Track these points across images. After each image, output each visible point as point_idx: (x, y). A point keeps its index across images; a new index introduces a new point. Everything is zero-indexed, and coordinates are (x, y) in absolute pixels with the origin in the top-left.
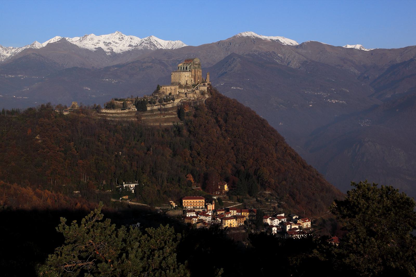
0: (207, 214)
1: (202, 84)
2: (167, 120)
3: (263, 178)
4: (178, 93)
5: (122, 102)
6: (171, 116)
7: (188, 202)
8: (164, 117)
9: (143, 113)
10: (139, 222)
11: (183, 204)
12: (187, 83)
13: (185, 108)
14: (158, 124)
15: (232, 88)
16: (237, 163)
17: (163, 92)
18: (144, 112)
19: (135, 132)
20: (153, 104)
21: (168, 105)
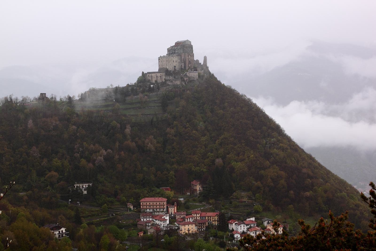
0: (163, 218)
4: (164, 81)
7: (146, 204)
10: (64, 228)
11: (142, 207)
12: (175, 69)
15: (299, 74)
17: (149, 81)
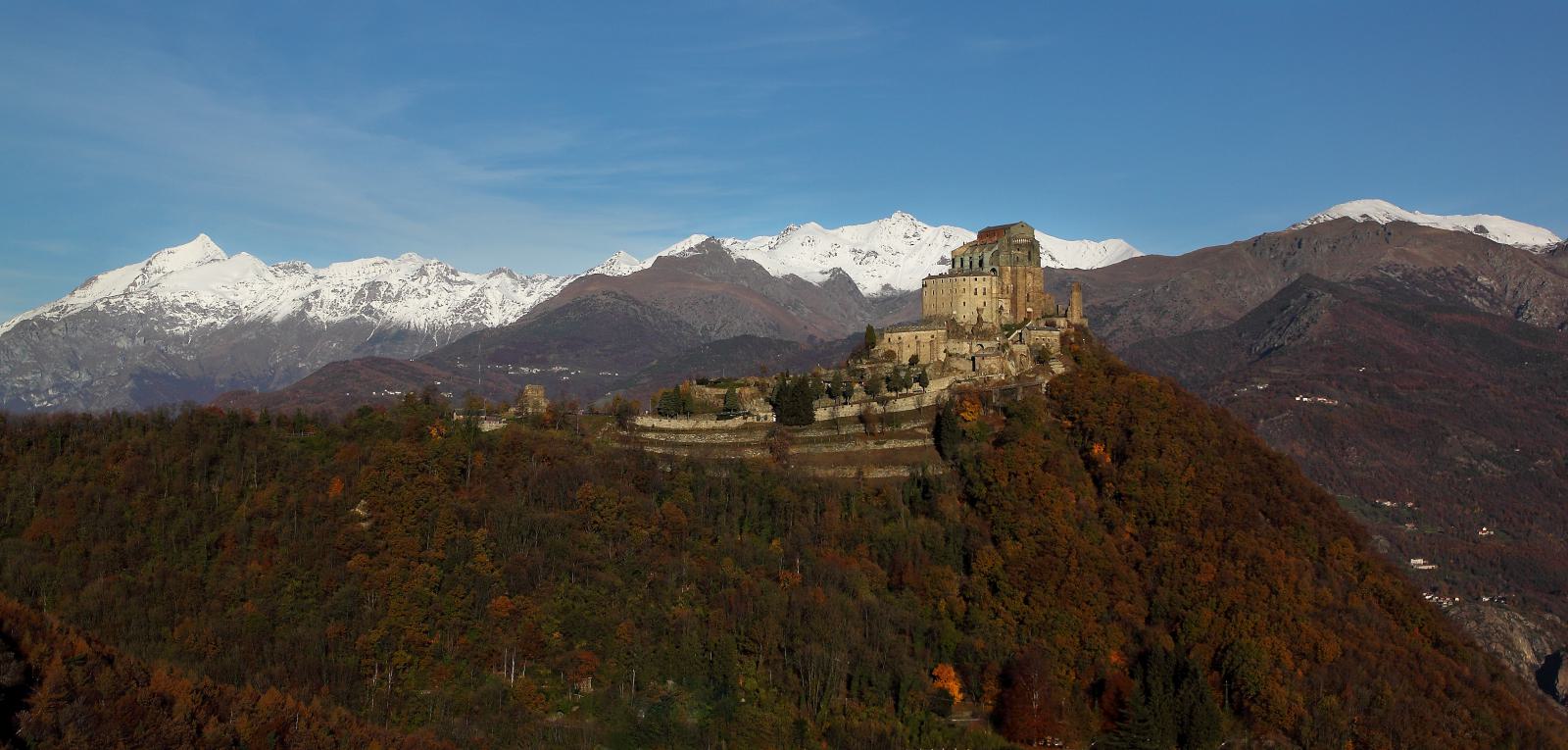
1: (1042, 324)
2: (888, 459)
3: (1244, 683)
4: (942, 357)
5: (723, 391)
6: (908, 444)
8: (879, 448)
9: (798, 431)
12: (979, 319)
13: (964, 411)
14: (851, 472)
16: (1148, 620)
17: (890, 355)
18: (803, 427)
19: (761, 499)
20: (843, 400)
21: (899, 402)
